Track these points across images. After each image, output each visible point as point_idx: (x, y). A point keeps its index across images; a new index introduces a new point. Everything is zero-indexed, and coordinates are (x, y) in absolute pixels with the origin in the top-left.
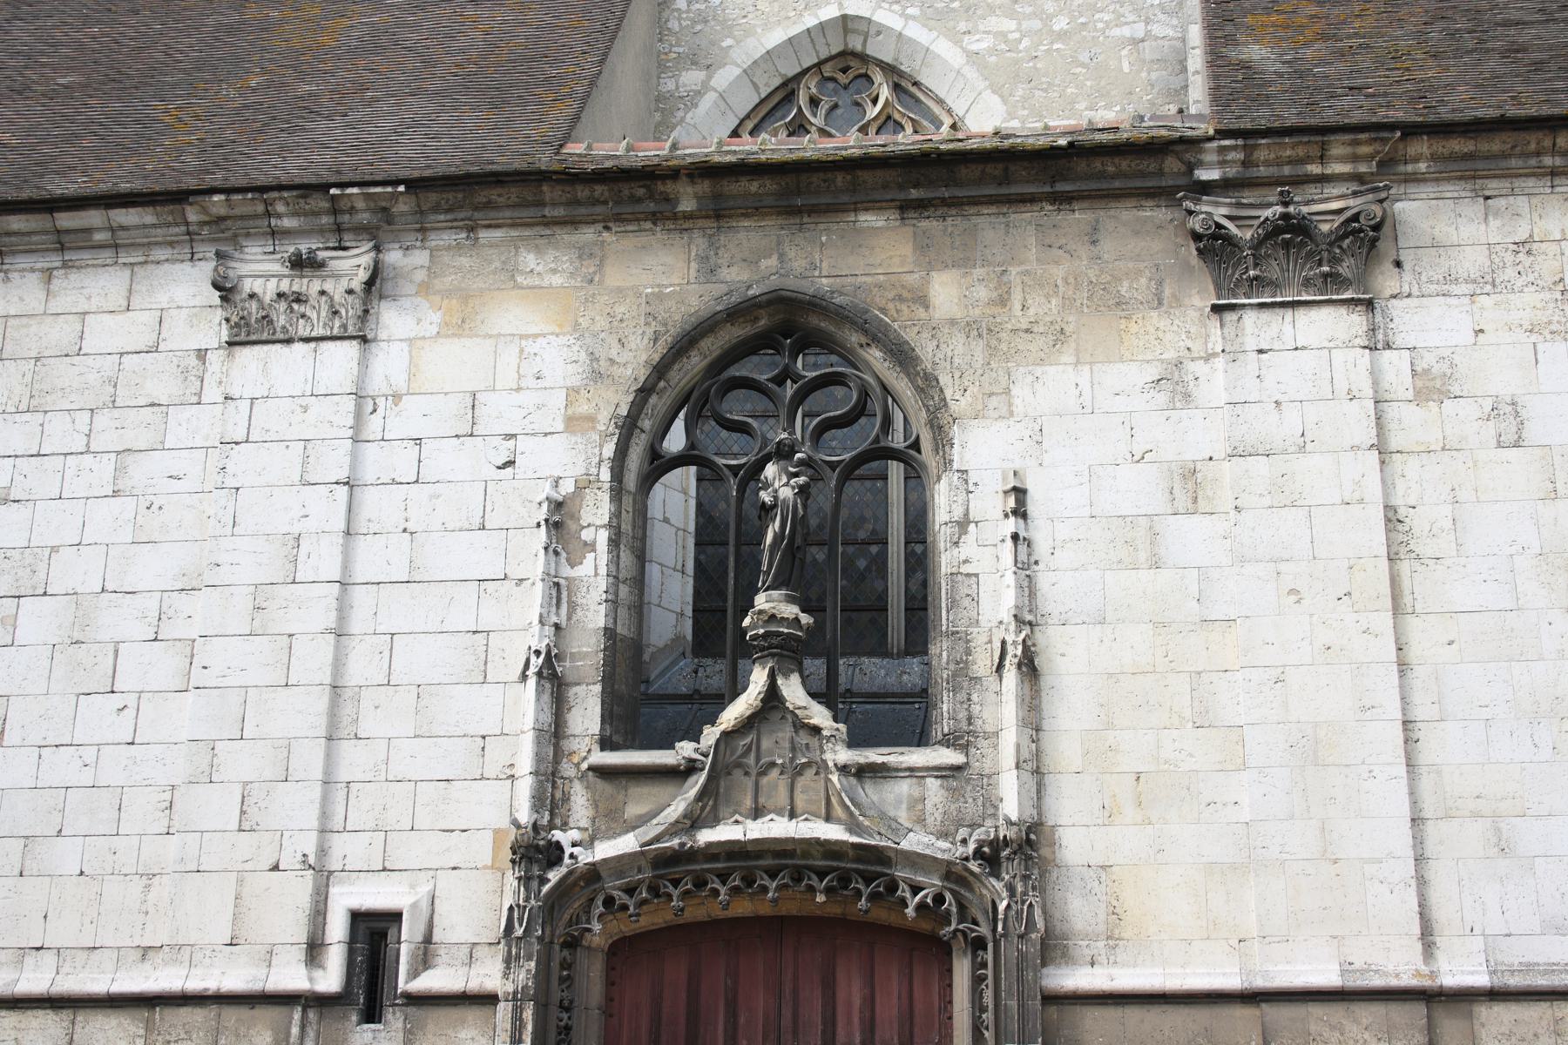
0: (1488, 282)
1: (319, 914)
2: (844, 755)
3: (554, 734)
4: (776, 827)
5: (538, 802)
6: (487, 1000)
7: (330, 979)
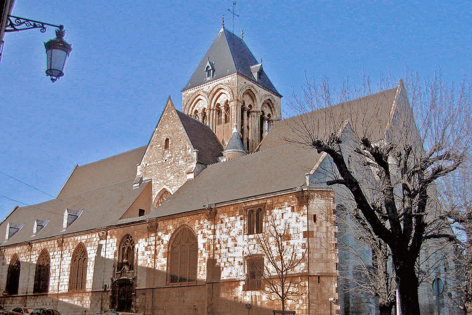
0: (163, 230)
1: (103, 285)
2: (127, 272)
3: (114, 271)
4: (125, 277)
5: (113, 276)
6: (110, 291)
7: (103, 290)
